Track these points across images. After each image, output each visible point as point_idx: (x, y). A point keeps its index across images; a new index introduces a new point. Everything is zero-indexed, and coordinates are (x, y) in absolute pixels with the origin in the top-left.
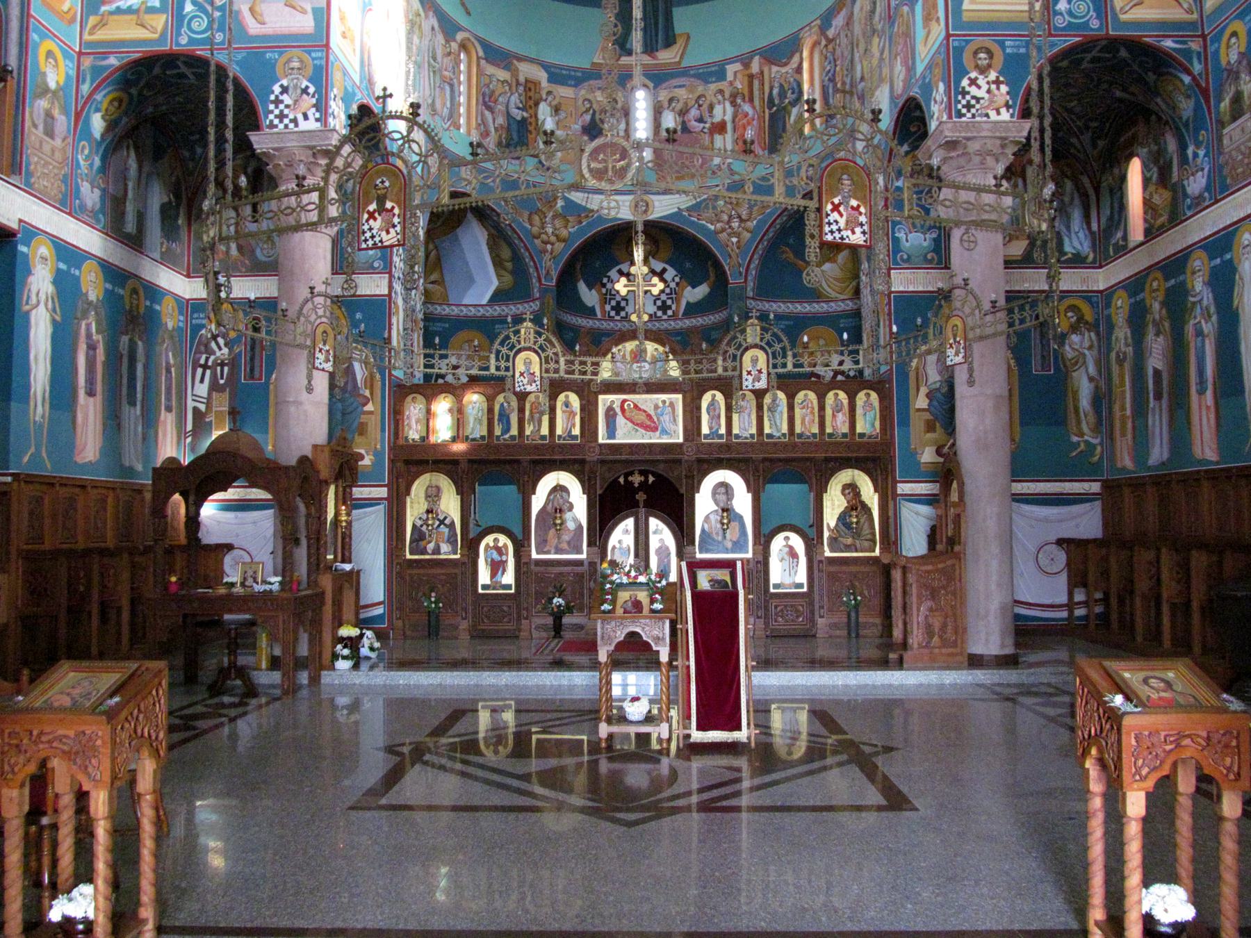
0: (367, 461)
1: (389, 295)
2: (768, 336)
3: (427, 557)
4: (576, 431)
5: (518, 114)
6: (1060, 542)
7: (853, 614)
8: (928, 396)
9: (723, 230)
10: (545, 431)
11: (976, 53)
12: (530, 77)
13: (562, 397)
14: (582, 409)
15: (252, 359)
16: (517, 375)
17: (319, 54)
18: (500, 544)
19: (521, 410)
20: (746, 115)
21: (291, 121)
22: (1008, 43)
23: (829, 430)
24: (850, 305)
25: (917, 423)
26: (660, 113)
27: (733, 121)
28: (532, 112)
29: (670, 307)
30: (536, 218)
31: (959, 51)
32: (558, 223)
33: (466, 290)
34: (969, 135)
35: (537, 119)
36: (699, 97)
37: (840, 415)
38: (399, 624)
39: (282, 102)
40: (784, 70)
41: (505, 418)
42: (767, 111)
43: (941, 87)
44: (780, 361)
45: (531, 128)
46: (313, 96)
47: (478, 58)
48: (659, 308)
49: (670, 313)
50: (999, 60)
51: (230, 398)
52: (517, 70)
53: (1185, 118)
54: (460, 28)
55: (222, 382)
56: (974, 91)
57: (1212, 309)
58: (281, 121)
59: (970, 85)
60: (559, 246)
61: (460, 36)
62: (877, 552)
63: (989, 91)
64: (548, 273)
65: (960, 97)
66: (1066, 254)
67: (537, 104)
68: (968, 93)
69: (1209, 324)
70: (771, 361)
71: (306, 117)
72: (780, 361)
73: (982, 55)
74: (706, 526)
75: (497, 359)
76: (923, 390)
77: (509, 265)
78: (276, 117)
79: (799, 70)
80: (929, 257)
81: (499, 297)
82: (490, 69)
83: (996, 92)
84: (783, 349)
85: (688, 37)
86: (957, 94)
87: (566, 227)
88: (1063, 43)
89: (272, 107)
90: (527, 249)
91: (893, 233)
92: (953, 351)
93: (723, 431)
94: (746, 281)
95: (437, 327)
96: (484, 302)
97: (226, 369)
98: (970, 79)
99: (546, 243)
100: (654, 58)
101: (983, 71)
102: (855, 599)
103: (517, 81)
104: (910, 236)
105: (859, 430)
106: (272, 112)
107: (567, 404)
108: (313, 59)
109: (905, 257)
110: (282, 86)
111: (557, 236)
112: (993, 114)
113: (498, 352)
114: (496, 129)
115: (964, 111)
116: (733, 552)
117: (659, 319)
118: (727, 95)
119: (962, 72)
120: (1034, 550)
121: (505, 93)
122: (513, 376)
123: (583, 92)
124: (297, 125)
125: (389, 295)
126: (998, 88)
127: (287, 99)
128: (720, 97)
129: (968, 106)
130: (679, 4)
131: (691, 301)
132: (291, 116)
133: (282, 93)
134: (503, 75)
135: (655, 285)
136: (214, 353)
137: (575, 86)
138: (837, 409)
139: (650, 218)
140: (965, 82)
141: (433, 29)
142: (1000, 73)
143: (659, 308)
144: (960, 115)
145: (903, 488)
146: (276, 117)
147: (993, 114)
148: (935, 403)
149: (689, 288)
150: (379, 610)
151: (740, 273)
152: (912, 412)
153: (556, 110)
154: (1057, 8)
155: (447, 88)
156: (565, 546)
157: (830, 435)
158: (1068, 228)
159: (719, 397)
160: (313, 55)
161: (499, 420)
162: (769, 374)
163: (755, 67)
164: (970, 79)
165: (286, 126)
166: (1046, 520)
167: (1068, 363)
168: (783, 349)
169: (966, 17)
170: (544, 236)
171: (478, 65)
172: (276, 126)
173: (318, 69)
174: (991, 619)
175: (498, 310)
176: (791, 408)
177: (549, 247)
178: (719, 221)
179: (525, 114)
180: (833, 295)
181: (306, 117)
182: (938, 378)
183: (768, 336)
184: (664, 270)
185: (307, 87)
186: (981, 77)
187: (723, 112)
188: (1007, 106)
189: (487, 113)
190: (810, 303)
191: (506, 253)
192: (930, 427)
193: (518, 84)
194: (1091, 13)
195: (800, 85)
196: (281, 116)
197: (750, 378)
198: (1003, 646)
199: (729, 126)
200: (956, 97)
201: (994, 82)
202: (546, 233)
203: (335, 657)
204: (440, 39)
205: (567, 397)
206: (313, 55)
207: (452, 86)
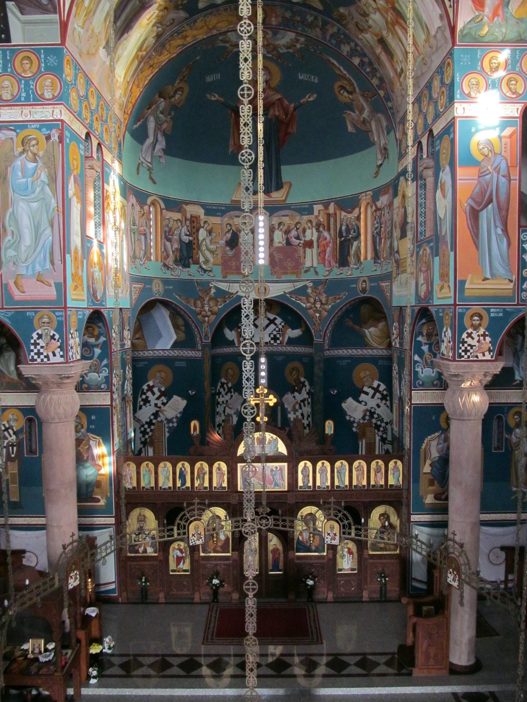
0: (102, 503)
1: (111, 405)
2: (340, 515)
3: (140, 555)
4: (225, 485)
5: (186, 239)
6: (503, 548)
7: (383, 588)
8: (430, 465)
9: (311, 308)
10: (206, 484)
11: (472, 316)
12: (194, 214)
13: (216, 465)
14: (228, 473)
15: (30, 440)
16: (191, 536)
17: (61, 314)
18: (181, 548)
19: (192, 473)
20: (325, 239)
21: (45, 357)
22: (492, 310)
23: (372, 483)
24: (385, 353)
25: (424, 481)
26: (273, 232)
27: (318, 241)
28: (195, 236)
29: (278, 339)
30: (199, 302)
31: (462, 315)
32: (212, 303)
33: (156, 342)
34: (465, 371)
35: (198, 240)
36: (298, 223)
37: (379, 474)
38: (125, 594)
39: (38, 344)
40: (349, 216)
41: (182, 476)
42: (338, 239)
43: (449, 333)
44: (347, 530)
45: (194, 246)
46: (58, 341)
47: (161, 210)
48: (272, 339)
49: (278, 342)
50: (486, 322)
51: (19, 464)
52: (185, 211)
54: (148, 195)
55: (13, 456)
56: (469, 341)
58: (39, 357)
59: (467, 337)
60: (213, 317)
61: (149, 201)
62: (398, 552)
63: (479, 341)
64: (206, 335)
65: (461, 345)
66: (516, 381)
67: (198, 231)
68: (466, 342)
70: (342, 530)
71: (54, 355)
72: (347, 530)
74: (300, 538)
75: (178, 529)
76: (428, 462)
77: (183, 328)
78: (36, 354)
79: (358, 218)
80: (435, 383)
81: (176, 345)
82: (169, 215)
83: (483, 341)
84: (349, 524)
85: (291, 185)
86: (459, 342)
87: (217, 305)
89: (32, 347)
90: (193, 322)
91: (414, 368)
93: (311, 484)
94: (324, 341)
95: (141, 365)
96: (168, 348)
97: (15, 448)
98: (467, 333)
99: (204, 317)
100: (270, 196)
101: (476, 328)
102: (385, 580)
103: (186, 218)
104: (424, 370)
105: (390, 483)
106: (32, 351)
107: (219, 469)
108: (57, 316)
109: (421, 383)
110: (38, 334)
111: (211, 311)
113: (179, 524)
114: (173, 252)
115: (463, 354)
116: (315, 552)
117: (272, 345)
118: (314, 224)
119: (463, 329)
120: (487, 551)
121: (178, 227)
122: (188, 537)
123: (226, 219)
124: (49, 360)
125: (111, 405)
126: (484, 339)
127: (41, 342)
128: (310, 225)
129: (466, 351)
130: (285, 164)
131: (291, 336)
132: (45, 354)
133: (38, 339)
134: (177, 216)
135: (271, 400)
136: (7, 439)
137: (221, 216)
138: (378, 470)
139: (267, 297)
140: (464, 335)
141: (133, 205)
142: (487, 329)
143: (272, 339)
144: (460, 356)
145: (414, 518)
146: (36, 354)
148: (435, 469)
149: (290, 330)
150: (113, 586)
151: (321, 336)
152: (421, 475)
153: (210, 232)
155: (143, 237)
156: (219, 549)
157: (373, 486)
158: (518, 365)
159: (309, 464)
160: (57, 314)
161: (179, 478)
162: (340, 537)
163: (332, 209)
164: (467, 333)
165: (42, 360)
166: (495, 535)
167: (513, 446)
168: (349, 524)
170: (203, 313)
171: (161, 214)
172: (36, 360)
173: (60, 323)
174: (463, 647)
175: (177, 353)
176: (351, 471)
177: (207, 319)
178: (308, 302)
179: (191, 238)
180: (376, 345)
181: (54, 355)
182: (437, 455)
183: (340, 515)
184: (275, 319)
185: (54, 335)
187: (311, 235)
188: (490, 351)
189: (168, 244)
190: (361, 349)
191: (181, 322)
192: (431, 483)
193: (186, 219)
195: (358, 228)
196: (39, 354)
197: (329, 537)
198: (469, 660)
199: (315, 244)
200: (458, 345)
201: (482, 335)
202: (205, 311)
203: (89, 677)
204: (138, 208)
205: (219, 464)
206: (57, 314)
207: (145, 235)
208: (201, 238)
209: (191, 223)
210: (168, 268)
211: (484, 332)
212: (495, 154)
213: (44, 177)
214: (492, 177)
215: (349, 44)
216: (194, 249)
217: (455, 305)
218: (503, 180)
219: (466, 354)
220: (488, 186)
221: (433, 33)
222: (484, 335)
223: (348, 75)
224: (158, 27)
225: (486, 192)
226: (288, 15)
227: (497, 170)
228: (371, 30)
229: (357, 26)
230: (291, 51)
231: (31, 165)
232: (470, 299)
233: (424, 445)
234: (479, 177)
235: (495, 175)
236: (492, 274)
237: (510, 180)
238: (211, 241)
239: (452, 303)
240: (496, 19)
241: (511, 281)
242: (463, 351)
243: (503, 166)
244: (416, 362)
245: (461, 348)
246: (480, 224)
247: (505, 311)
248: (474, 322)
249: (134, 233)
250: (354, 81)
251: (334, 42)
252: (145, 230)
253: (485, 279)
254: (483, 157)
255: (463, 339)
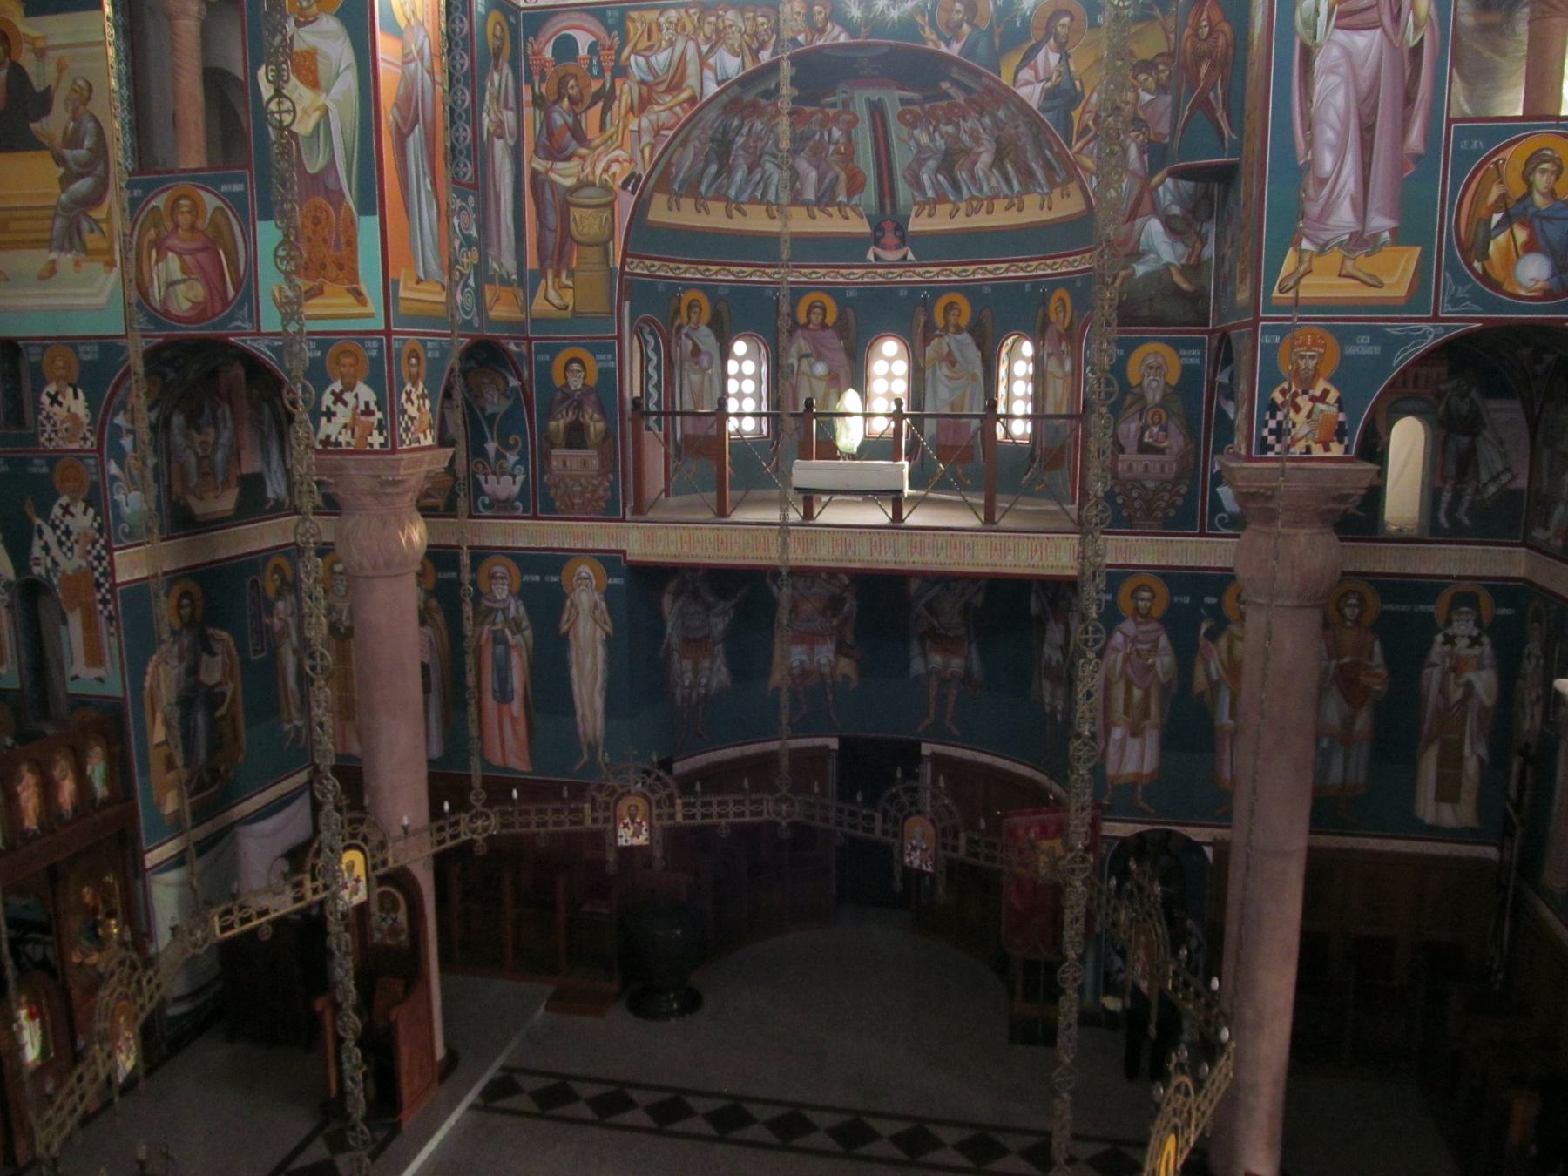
22: (429, 345)
53: (489, 411)
57: (525, 623)
69: (519, 637)
91: (112, 495)
92: (630, 832)
158: (268, 465)
162: (368, 879)
192: (170, 764)
217: (387, 332)
233: (148, 678)
239: (382, 327)
244: (114, 478)
253: (419, 281)
255: (328, 408)
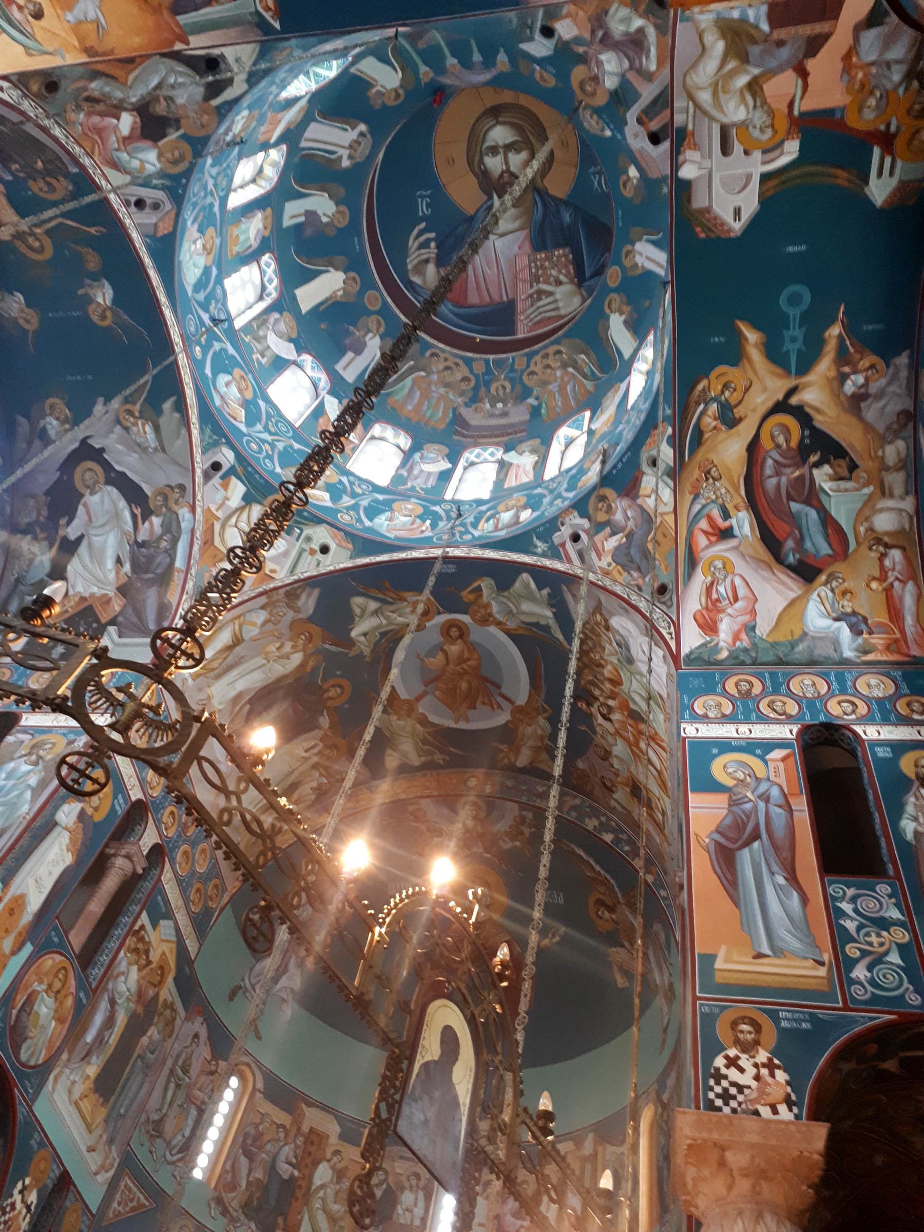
5: (285, 1170)
11: (734, 1024)
12: (319, 1128)
22: (782, 1015)
45: (299, 1193)
50: (770, 1035)
59: (727, 1067)
65: (712, 1082)
67: (316, 1164)
68: (725, 1077)
73: (745, 1027)
82: (266, 1107)
88: (865, 1021)
98: (727, 1057)
101: (749, 1048)
103: (299, 1129)
112: (765, 1112)
114: (249, 1183)
115: (719, 1102)
119: (713, 1047)
126: (772, 1075)
129: (726, 1097)
140: (719, 1062)
142: (775, 1053)
147: (765, 1112)
154: (853, 975)
155: (194, 1112)
164: (727, 1057)
169: (719, 978)
179: (296, 1173)
186: (744, 1056)
188: (790, 1104)
189: (243, 1160)
194: (906, 984)
200: (705, 1082)
201: (764, 1065)
208: (317, 1181)
209: (305, 1143)
210: (225, 1212)
211: (770, 1060)
212: (757, 778)
213: (33, 781)
214: (755, 807)
215: (597, 818)
216: (297, 1199)
218: (778, 813)
219: (726, 1104)
220: (748, 817)
221: (665, 696)
222: (770, 1066)
223: (602, 872)
224: (321, 775)
225: (745, 825)
226: (509, 783)
227: (765, 797)
228: (619, 779)
229: (605, 785)
230: (518, 843)
231: (26, 768)
232: (727, 988)
234: (730, 805)
235: (762, 805)
236: (772, 947)
237: (791, 811)
238: (336, 1193)
240: (738, 644)
241: (822, 964)
242: (718, 1096)
243: (775, 792)
245: (712, 1089)
246: (739, 869)
247: (813, 1018)
248: (741, 1036)
249: (178, 1086)
250: (612, 881)
251: (574, 814)
252: (203, 1102)
253: (760, 956)
254: (735, 782)
